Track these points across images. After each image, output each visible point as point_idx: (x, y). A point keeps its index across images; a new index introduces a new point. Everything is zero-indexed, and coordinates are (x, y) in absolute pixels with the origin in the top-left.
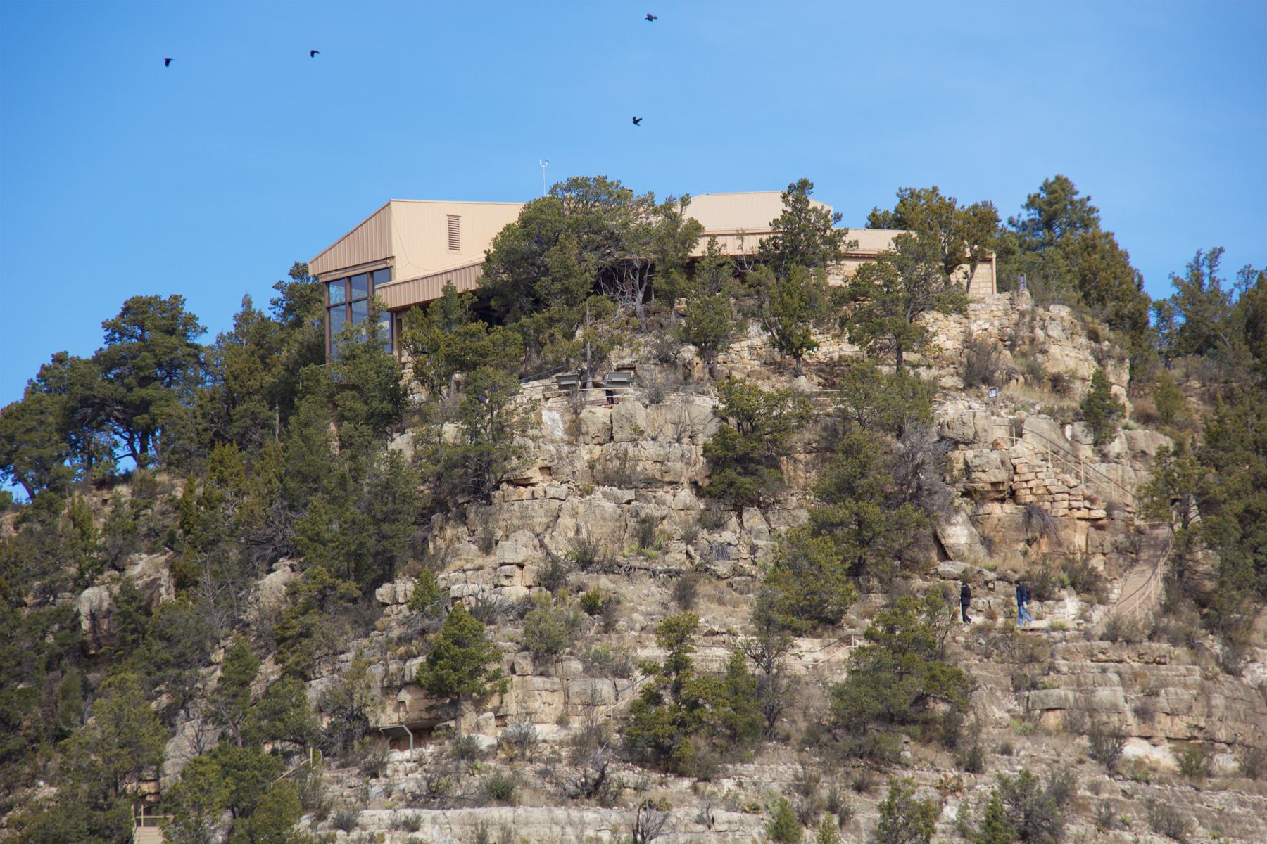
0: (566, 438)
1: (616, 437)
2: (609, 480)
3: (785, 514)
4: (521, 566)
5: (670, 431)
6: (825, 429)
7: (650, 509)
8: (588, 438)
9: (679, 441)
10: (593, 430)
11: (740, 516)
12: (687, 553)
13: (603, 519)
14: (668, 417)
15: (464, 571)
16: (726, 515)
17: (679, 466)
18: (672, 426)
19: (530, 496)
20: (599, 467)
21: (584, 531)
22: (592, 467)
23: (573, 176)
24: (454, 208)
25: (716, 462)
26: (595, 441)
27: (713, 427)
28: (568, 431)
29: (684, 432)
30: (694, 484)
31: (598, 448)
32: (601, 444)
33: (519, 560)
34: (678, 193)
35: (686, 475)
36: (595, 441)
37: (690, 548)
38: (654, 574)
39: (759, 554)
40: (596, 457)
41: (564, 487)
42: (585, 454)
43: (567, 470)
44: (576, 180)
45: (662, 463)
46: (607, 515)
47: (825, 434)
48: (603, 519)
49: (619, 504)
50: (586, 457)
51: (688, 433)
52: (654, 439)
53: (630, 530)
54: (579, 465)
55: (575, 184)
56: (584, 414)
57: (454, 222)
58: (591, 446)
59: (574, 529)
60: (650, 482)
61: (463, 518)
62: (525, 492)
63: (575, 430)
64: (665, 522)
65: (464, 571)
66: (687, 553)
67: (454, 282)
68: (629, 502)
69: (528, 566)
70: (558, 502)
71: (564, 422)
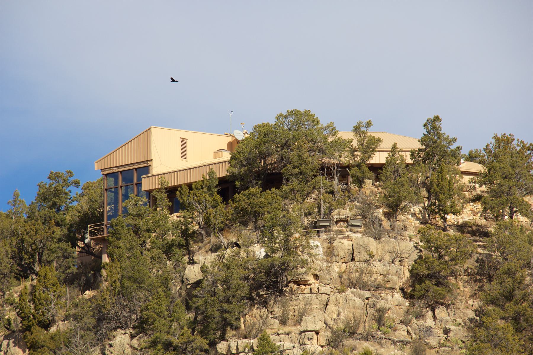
0: (325, 258)
1: (356, 259)
2: (352, 285)
3: (458, 311)
4: (317, 333)
5: (387, 258)
6: (477, 261)
7: (381, 304)
8: (338, 259)
9: (393, 262)
10: (342, 254)
11: (433, 311)
12: (408, 332)
13: (354, 308)
14: (387, 248)
15: (278, 334)
16: (424, 310)
17: (395, 278)
18: (393, 254)
19: (309, 291)
20: (345, 277)
21: (342, 314)
22: (340, 276)
23: (290, 109)
24: (184, 134)
25: (416, 278)
26: (342, 261)
27: (415, 256)
28: (326, 254)
29: (397, 258)
30: (402, 290)
31: (344, 265)
32: (346, 263)
33: (317, 328)
34: (365, 121)
35: (400, 284)
36: (343, 261)
37: (409, 328)
38: (394, 343)
39: (451, 334)
40: (343, 270)
41: (328, 287)
42: (337, 268)
43: (328, 277)
44: (292, 112)
45: (385, 276)
46: (356, 306)
47: (477, 264)
48: (354, 308)
49: (363, 300)
50: (337, 270)
51: (399, 259)
52: (380, 261)
53: (370, 316)
54: (334, 275)
55: (291, 113)
56: (335, 243)
57: (184, 142)
58: (340, 263)
59: (336, 313)
60: (378, 287)
61: (264, 304)
62: (307, 289)
63: (330, 253)
64: (389, 312)
65: (278, 334)
66: (408, 332)
67: (214, 169)
68: (367, 299)
69: (321, 333)
70: (327, 296)
71: (323, 248)
